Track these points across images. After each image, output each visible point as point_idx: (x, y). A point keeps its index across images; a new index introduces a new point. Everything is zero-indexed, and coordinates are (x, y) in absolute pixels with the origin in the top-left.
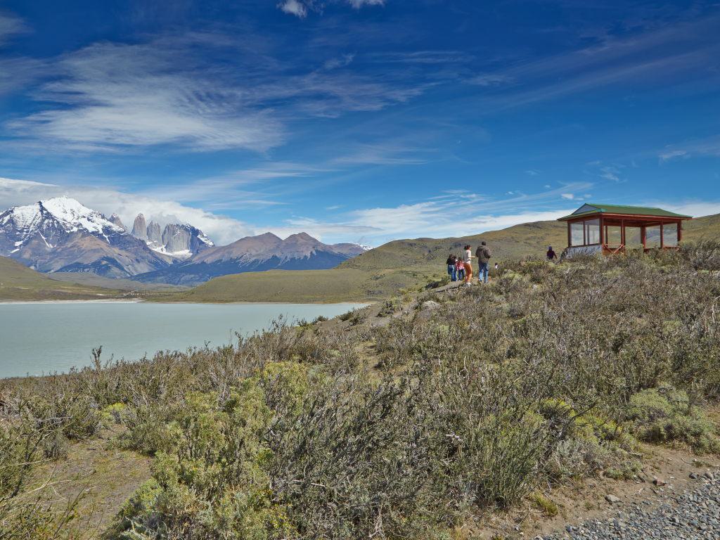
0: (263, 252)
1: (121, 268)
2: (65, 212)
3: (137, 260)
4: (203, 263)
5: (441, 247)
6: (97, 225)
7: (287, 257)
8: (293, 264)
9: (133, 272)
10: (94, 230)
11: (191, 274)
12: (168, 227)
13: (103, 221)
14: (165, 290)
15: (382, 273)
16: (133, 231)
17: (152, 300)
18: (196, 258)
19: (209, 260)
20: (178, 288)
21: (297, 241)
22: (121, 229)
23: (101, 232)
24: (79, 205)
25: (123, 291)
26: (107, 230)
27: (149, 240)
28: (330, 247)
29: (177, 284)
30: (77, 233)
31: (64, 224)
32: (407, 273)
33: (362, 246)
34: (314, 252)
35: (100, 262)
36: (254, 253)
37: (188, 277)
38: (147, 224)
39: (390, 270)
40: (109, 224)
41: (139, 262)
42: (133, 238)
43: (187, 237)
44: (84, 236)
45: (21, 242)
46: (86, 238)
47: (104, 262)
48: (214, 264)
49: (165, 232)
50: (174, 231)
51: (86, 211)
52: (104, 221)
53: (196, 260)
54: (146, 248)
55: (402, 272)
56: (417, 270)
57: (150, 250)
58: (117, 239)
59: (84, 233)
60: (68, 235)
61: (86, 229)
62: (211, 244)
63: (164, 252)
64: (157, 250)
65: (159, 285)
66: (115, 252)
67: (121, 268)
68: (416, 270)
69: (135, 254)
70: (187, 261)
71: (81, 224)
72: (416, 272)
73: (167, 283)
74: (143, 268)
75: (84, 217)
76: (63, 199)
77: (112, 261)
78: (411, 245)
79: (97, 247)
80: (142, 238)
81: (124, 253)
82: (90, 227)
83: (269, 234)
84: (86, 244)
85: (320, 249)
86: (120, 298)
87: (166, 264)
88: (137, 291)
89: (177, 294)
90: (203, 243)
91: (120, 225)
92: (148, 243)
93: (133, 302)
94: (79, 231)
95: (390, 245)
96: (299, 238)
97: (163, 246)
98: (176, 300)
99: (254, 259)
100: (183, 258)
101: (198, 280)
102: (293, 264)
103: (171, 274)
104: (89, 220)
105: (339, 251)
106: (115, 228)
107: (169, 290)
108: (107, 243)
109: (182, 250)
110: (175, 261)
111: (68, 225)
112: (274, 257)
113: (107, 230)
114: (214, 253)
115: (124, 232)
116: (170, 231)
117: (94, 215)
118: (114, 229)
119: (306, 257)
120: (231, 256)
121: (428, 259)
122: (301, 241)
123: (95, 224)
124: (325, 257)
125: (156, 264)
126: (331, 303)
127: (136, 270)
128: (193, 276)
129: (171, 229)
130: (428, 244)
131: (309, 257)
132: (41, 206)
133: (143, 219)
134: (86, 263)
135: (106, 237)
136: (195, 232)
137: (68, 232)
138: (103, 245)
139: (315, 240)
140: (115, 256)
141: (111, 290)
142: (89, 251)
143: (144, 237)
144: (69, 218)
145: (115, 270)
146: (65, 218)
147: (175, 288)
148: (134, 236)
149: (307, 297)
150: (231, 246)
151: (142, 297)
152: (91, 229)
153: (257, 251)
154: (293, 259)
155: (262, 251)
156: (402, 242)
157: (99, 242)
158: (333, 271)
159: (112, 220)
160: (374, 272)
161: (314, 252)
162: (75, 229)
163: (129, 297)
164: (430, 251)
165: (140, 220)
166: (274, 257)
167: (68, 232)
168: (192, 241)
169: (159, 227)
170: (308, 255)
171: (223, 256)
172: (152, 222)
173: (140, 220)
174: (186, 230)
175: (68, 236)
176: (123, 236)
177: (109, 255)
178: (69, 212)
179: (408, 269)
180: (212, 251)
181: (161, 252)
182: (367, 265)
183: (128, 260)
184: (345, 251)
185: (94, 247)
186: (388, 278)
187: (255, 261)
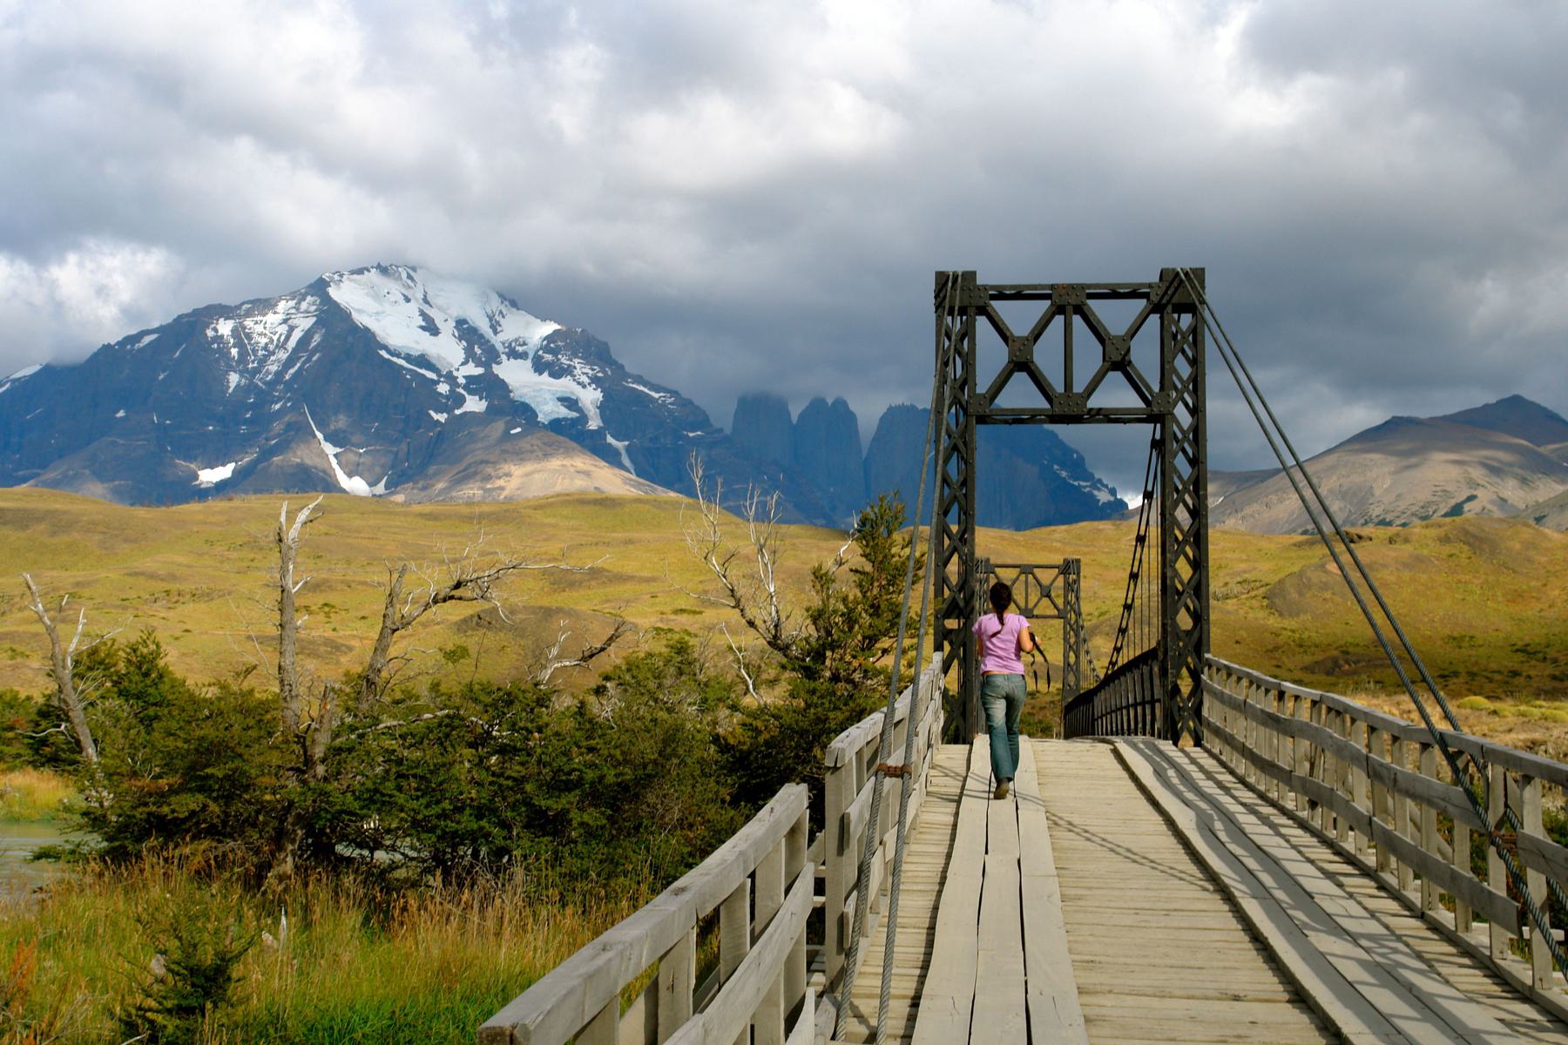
2: (431, 328)
10: (563, 412)
23: (594, 424)
45: (224, 472)
75: (513, 354)
104: (539, 366)
132: (327, 300)
137: (442, 417)
144: (448, 351)
162: (474, 404)
167: (442, 417)
178: (447, 329)
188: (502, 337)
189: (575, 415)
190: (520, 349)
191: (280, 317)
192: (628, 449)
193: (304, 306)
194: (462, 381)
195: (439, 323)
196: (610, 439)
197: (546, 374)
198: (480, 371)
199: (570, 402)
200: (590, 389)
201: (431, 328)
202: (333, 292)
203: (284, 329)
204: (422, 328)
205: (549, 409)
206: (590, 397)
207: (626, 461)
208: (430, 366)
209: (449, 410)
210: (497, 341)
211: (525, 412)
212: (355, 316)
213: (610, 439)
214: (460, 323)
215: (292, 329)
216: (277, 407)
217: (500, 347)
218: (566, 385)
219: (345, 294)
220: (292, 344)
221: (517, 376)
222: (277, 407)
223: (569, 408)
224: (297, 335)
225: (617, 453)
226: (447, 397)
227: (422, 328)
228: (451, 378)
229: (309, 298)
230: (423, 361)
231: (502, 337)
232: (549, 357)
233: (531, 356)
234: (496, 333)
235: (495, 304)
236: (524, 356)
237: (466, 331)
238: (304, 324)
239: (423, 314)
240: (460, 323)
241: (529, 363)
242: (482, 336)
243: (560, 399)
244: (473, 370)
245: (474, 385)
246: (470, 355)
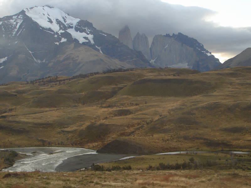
2: (51, 21)
23: (92, 42)
75: (71, 27)
104: (77, 30)
135: (99, 48)
144: (55, 27)
162: (63, 40)
178: (54, 21)
188: (67, 23)
189: (88, 41)
190: (71, 26)
191: (14, 20)
192: (101, 48)
193: (19, 17)
194: (60, 34)
195: (52, 20)
196: (97, 47)
197: (79, 32)
198: (63, 31)
199: (85, 38)
200: (90, 35)
201: (51, 21)
202: (27, 14)
203: (15, 23)
204: (48, 21)
205: (81, 40)
206: (90, 37)
207: (101, 52)
208: (53, 31)
210: (65, 24)
211: (76, 41)
212: (33, 19)
213: (97, 47)
214: (57, 20)
215: (17, 23)
216: (16, 42)
217: (66, 25)
218: (84, 34)
219: (28, 14)
220: (18, 27)
221: (72, 32)
222: (16, 42)
223: (86, 39)
224: (19, 25)
226: (57, 38)
227: (48, 21)
228: (57, 33)
229: (20, 15)
230: (50, 29)
231: (67, 23)
233: (74, 27)
234: (65, 22)
235: (64, 15)
236: (72, 27)
237: (58, 22)
238: (20, 22)
239: (48, 18)
240: (57, 20)
241: (74, 29)
242: (62, 23)
243: (84, 37)
244: (62, 31)
245: (63, 35)
246: (61, 28)
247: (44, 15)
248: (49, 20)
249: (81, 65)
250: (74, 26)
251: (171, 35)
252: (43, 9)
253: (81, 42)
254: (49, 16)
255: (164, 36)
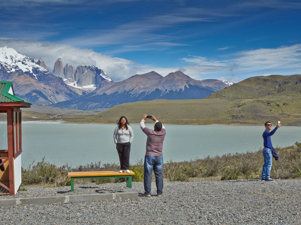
0: (150, 87)
1: (46, 98)
3: (57, 92)
4: (105, 94)
5: (289, 82)
6: (28, 67)
7: (166, 90)
8: (171, 95)
9: (55, 101)
10: (27, 70)
11: (96, 102)
12: (78, 68)
13: (33, 64)
14: (78, 114)
15: (243, 102)
16: (54, 71)
17: (71, 122)
18: (100, 90)
19: (109, 92)
20: (87, 112)
21: (175, 78)
22: (45, 70)
24: (16, 52)
25: (49, 115)
26: (35, 70)
27: (66, 77)
28: (200, 82)
29: (85, 110)
30: (15, 73)
31: (6, 66)
32: (263, 102)
33: (223, 81)
34: (187, 86)
35: (31, 94)
36: (142, 86)
37: (94, 104)
38: (64, 66)
39: (250, 100)
40: (37, 66)
41: (58, 94)
42: (54, 76)
43: (92, 75)
44: (19, 75)
46: (21, 77)
47: (34, 94)
48: (112, 95)
49: (76, 72)
50: (83, 71)
51: (21, 57)
52: (34, 64)
53: (100, 92)
54: (63, 83)
55: (259, 101)
56: (271, 100)
57: (66, 85)
58: (43, 77)
59: (20, 72)
60: (9, 75)
61: (21, 70)
62: (110, 80)
63: (76, 86)
64: (71, 84)
65: (74, 110)
66: (41, 86)
67: (46, 98)
68: (269, 100)
69: (56, 88)
70: (92, 93)
71: (17, 67)
72: (270, 101)
73: (78, 109)
74: (62, 98)
75: (19, 61)
76: (5, 48)
77: (40, 93)
78: (265, 80)
79: (29, 83)
80: (61, 76)
81: (48, 87)
82: (24, 68)
83: (153, 72)
84: (21, 80)
85: (191, 83)
86: (48, 120)
87: (77, 95)
88: (59, 114)
89: (88, 117)
90: (104, 79)
91: (44, 66)
92: (65, 80)
93: (58, 123)
94: (16, 71)
95: (248, 80)
96: (176, 75)
97: (75, 82)
98: (89, 121)
99: (142, 91)
100: (90, 91)
101: (101, 107)
102: (171, 95)
103: (81, 103)
104: (23, 63)
105: (207, 85)
106: (42, 69)
107: (81, 114)
108: (36, 80)
109: (89, 84)
110: (84, 93)
111: (9, 67)
112: (157, 90)
113: (35, 70)
114: (112, 87)
115: (48, 71)
116: (80, 72)
117: (27, 60)
118: (40, 70)
119: (181, 90)
120: (125, 89)
121: (279, 91)
122: (177, 77)
123: (27, 67)
124: (196, 90)
125: (70, 95)
126: (204, 124)
127: (56, 100)
128: (97, 104)
129: (81, 69)
130: (278, 80)
131: (184, 90)
133: (61, 62)
134: (21, 94)
135: (35, 75)
136: (98, 71)
137: (9, 72)
138: (33, 81)
139: (188, 77)
140: (41, 89)
141: (41, 114)
142: (23, 85)
143: (62, 76)
144: (9, 62)
145: (41, 99)
146: (7, 62)
147: (85, 113)
148: (55, 75)
149: (186, 120)
150: (125, 82)
151: (64, 119)
152: (24, 70)
153: (144, 85)
154: (171, 91)
155: (148, 85)
156: (258, 78)
157: (30, 79)
158: (206, 101)
159: (39, 63)
160: (237, 101)
161: (187, 86)
162: (13, 70)
163: (54, 119)
164: (280, 85)
165: (58, 63)
166: (157, 90)
167: (9, 72)
168: (96, 78)
169: (72, 67)
170: (183, 88)
171: (119, 89)
172: (67, 64)
173: (58, 63)
174: (92, 70)
175: (9, 75)
176: (47, 75)
177: (37, 89)
178: (9, 58)
179: (263, 99)
180: (111, 85)
181: (73, 86)
182: (231, 96)
183: (50, 92)
184: (211, 85)
185: (27, 83)
186: (248, 105)
187: (143, 92)
189: (28, 71)
190: (20, 60)
192: (37, 76)
194: (11, 66)
196: (34, 74)
206: (31, 69)
209: (10, 71)
213: (34, 74)
221: (20, 65)
225: (35, 76)
232: (24, 62)
233: (21, 61)
237: (12, 58)
241: (21, 63)
247: (3, 53)
248: (5, 57)
249: (20, 86)
250: (21, 60)
251: (88, 66)
252: (3, 49)
253: (24, 72)
254: (5, 54)
255: (84, 67)
